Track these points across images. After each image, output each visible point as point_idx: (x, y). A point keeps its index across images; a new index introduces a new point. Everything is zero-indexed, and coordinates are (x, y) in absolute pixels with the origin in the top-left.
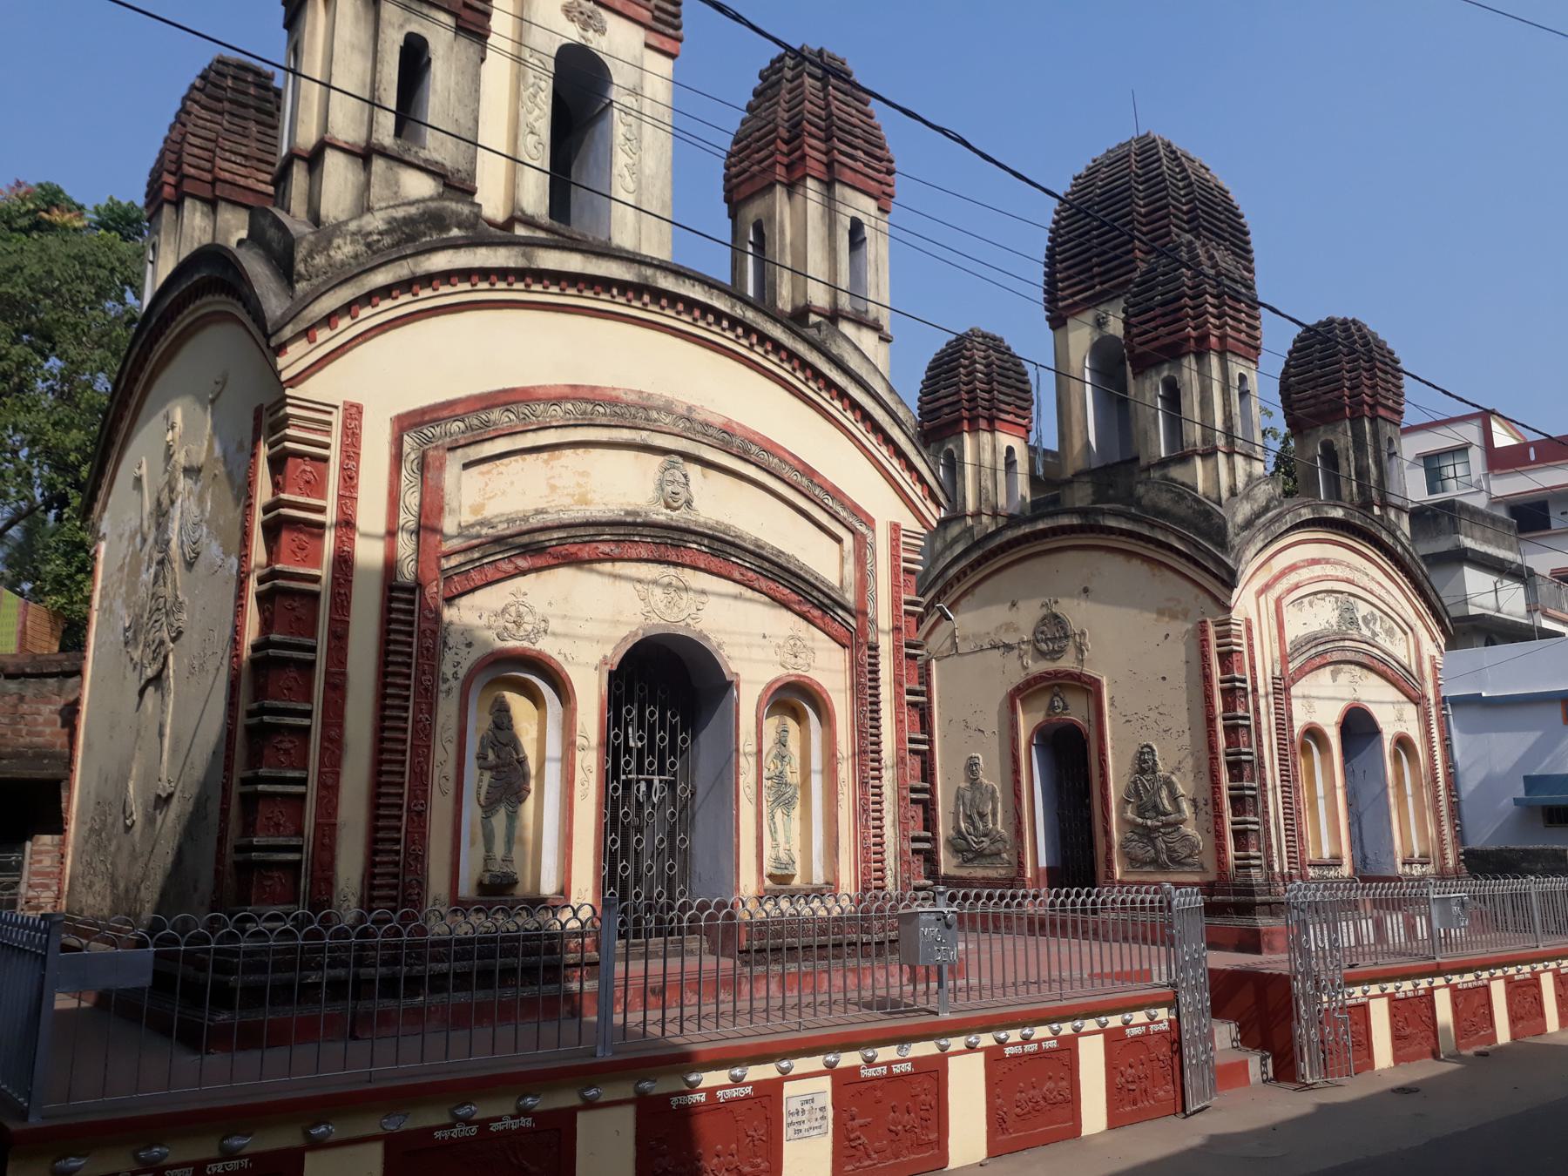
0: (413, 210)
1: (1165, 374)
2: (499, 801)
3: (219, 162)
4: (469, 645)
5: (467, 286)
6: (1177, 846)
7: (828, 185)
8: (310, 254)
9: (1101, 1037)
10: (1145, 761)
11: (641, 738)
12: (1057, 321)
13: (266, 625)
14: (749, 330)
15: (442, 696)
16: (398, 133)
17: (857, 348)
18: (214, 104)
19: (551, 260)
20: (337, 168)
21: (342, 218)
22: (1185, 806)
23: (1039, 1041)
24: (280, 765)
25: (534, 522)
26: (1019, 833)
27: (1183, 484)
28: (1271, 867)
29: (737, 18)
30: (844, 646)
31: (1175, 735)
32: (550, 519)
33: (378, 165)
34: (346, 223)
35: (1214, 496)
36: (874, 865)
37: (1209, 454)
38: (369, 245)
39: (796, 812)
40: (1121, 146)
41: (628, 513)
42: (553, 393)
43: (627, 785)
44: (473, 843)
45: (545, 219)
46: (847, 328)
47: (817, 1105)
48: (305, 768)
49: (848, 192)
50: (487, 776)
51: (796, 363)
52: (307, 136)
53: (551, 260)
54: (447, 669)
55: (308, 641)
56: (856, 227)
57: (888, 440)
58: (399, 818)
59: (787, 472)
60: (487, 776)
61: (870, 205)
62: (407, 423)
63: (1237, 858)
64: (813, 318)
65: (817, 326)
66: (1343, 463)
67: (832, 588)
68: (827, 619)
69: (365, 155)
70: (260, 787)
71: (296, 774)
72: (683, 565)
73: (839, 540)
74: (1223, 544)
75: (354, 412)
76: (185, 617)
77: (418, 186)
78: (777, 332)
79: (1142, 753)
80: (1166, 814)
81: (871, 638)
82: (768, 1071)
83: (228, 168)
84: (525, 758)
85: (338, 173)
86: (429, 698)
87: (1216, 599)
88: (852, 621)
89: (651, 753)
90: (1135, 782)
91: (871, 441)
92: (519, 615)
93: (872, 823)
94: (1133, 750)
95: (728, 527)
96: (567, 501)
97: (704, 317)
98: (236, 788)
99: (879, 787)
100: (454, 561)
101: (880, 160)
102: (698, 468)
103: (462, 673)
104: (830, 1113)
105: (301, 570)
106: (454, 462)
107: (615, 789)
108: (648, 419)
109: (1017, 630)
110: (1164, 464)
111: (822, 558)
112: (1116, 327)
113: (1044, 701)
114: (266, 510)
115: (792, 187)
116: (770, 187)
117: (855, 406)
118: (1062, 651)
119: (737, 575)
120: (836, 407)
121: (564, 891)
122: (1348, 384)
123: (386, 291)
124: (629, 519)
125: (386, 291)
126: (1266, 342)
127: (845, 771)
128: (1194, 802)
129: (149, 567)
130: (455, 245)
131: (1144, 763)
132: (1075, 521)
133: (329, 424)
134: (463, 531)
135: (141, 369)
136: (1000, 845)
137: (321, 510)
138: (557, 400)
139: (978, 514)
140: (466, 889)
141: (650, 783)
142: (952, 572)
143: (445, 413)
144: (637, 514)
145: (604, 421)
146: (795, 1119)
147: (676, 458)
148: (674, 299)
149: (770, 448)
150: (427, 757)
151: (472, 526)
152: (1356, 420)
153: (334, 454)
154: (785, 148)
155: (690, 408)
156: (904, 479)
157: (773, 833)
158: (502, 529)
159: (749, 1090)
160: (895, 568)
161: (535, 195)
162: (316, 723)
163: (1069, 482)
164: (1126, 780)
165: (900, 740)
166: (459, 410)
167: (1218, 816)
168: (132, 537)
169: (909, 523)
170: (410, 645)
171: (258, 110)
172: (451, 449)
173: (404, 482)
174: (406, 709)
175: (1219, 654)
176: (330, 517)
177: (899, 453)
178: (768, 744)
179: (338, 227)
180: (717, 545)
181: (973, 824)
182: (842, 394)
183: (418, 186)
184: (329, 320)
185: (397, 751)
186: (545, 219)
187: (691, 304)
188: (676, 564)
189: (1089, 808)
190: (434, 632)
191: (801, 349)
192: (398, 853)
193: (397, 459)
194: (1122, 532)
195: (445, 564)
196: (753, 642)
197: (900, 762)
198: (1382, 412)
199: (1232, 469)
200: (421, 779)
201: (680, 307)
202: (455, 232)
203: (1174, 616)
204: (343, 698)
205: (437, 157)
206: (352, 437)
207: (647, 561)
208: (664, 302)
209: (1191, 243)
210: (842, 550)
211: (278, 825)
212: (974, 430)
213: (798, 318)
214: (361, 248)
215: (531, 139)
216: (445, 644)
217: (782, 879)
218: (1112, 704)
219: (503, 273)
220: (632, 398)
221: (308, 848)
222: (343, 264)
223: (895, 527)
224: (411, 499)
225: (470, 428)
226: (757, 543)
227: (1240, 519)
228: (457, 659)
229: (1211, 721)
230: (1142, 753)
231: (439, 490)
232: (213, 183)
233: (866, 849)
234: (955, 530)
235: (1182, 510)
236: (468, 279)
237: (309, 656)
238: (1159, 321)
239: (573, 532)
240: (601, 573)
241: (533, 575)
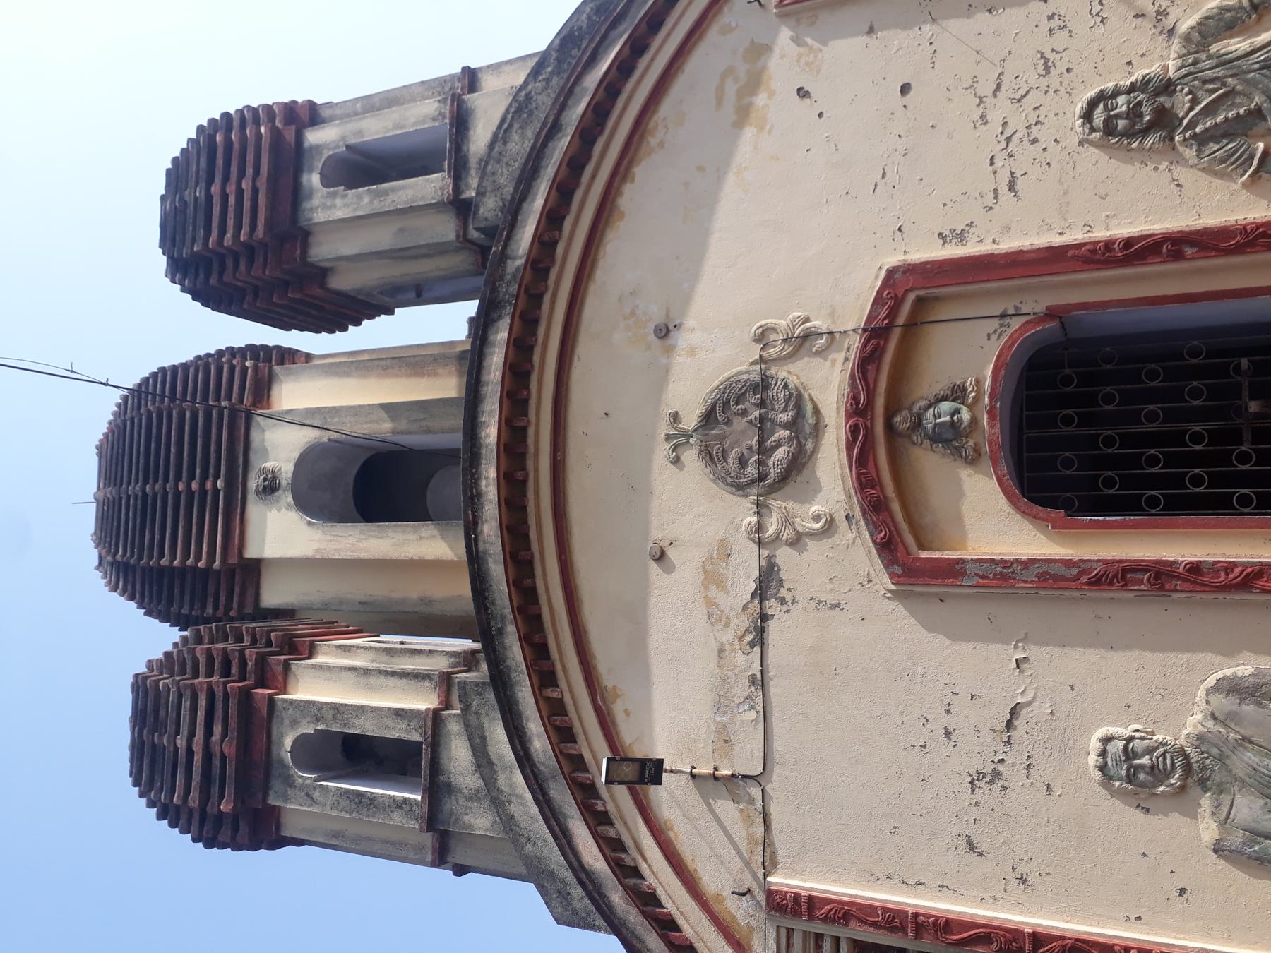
1: (315, 179)
10: (1134, 113)
31: (1061, 39)
90: (1201, 140)
94: (1098, 164)
113: (930, 464)
118: (797, 400)
142: (540, 744)
164: (1191, 178)
203: (754, 83)
218: (961, 237)
230: (1109, 129)
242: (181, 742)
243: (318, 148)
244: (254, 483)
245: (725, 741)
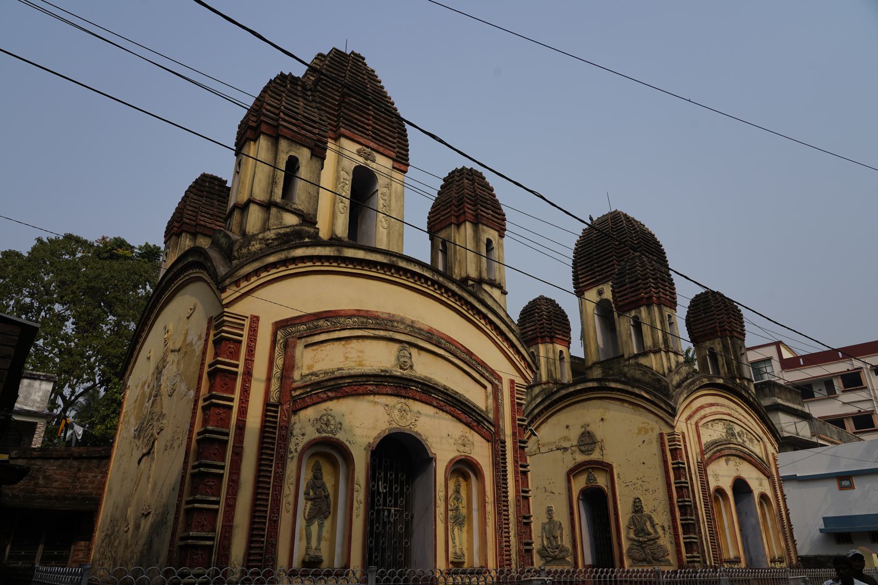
0: (288, 230)
2: (314, 517)
3: (199, 217)
4: (303, 435)
5: (311, 264)
6: (656, 551)
7: (475, 224)
8: (240, 248)
11: (385, 488)
12: (580, 292)
13: (205, 422)
14: (441, 286)
15: (289, 460)
16: (283, 197)
17: (491, 296)
18: (199, 193)
19: (350, 253)
20: (255, 212)
21: (256, 232)
22: (659, 530)
24: (207, 494)
25: (337, 374)
26: (574, 546)
27: (646, 366)
28: (705, 562)
29: (441, 141)
30: (488, 441)
32: (345, 372)
33: (274, 211)
34: (257, 235)
35: (661, 372)
36: (505, 557)
37: (657, 351)
38: (267, 245)
39: (465, 529)
40: (604, 216)
41: (382, 371)
42: (349, 313)
44: (300, 540)
45: (346, 239)
46: (487, 288)
48: (219, 496)
49: (485, 228)
50: (309, 503)
52: (245, 197)
53: (350, 253)
54: (292, 447)
55: (225, 430)
56: (489, 242)
57: (507, 339)
58: (265, 523)
59: (459, 353)
60: (309, 503)
61: (496, 234)
62: (280, 325)
63: (687, 557)
64: (470, 282)
65: (472, 286)
66: (720, 358)
67: (482, 411)
68: (480, 427)
69: (267, 206)
70: (196, 505)
71: (215, 499)
72: (409, 398)
73: (485, 387)
74: (668, 395)
75: (255, 320)
76: (165, 421)
77: (291, 220)
78: (454, 288)
79: (635, 502)
80: (650, 534)
81: (502, 437)
83: (203, 220)
84: (329, 495)
85: (255, 215)
86: (282, 462)
87: (667, 422)
88: (492, 428)
89: (391, 495)
91: (499, 340)
92: (328, 420)
93: (504, 535)
95: (431, 379)
96: (353, 364)
97: (420, 280)
98: (184, 506)
99: (508, 515)
100: (298, 393)
101: (499, 214)
103: (299, 449)
105: (225, 395)
107: (372, 514)
108: (392, 326)
109: (569, 440)
110: (636, 356)
111: (476, 395)
112: (608, 294)
114: (210, 366)
115: (458, 226)
116: (450, 225)
117: (491, 322)
119: (435, 403)
120: (482, 323)
121: (347, 566)
123: (274, 265)
124: (383, 374)
125: (274, 265)
126: (679, 300)
127: (490, 508)
128: (663, 528)
129: (149, 399)
130: (307, 245)
131: (637, 507)
132: (595, 384)
133: (243, 325)
134: (303, 376)
135: (155, 307)
136: (564, 553)
137: (237, 366)
138: (350, 316)
139: (547, 383)
140: (296, 564)
141: (389, 511)
142: (536, 411)
143: (298, 321)
144: (386, 371)
145: (372, 326)
147: (406, 345)
148: (406, 271)
149: (451, 341)
150: (280, 492)
151: (308, 375)
153: (245, 340)
154: (456, 209)
155: (412, 321)
156: (516, 358)
157: (453, 539)
158: (322, 377)
160: (512, 402)
161: (342, 229)
162: (226, 472)
163: (591, 368)
165: (517, 491)
166: (304, 320)
167: (676, 536)
168: (143, 386)
169: (519, 380)
170: (275, 433)
171: (219, 196)
172: (300, 338)
173: (276, 354)
174: (271, 466)
175: (670, 450)
176: (240, 370)
177: (512, 345)
178: (450, 492)
179: (254, 235)
180: (425, 388)
181: (550, 542)
182: (485, 317)
183: (291, 220)
184: (247, 277)
185: (264, 494)
186: (346, 239)
187: (414, 274)
188: (405, 397)
189: (610, 532)
190: (286, 427)
191: (465, 295)
192: (263, 542)
193: (274, 342)
194: (618, 390)
195: (294, 394)
196: (443, 437)
198: (735, 334)
199: (669, 359)
200: (277, 502)
201: (409, 275)
202: (307, 240)
204: (241, 460)
205: (300, 208)
206: (253, 331)
207: (391, 395)
208: (401, 273)
209: (640, 256)
210: (486, 392)
211: (203, 525)
212: (544, 342)
213: (463, 282)
214: (263, 246)
215: (341, 205)
216: (292, 434)
217: (458, 564)
220: (385, 316)
221: (218, 538)
222: (255, 252)
224: (279, 362)
225: (309, 328)
226: (445, 387)
227: (674, 383)
228: (297, 441)
229: (669, 485)
231: (293, 357)
232: (196, 226)
233: (501, 548)
234: (537, 390)
235: (646, 379)
236: (312, 261)
237: (225, 438)
238: (629, 290)
239: (355, 380)
240: (369, 401)
241: (335, 401)
242: (527, 325)
243: (640, 312)
244: (600, 287)
245: (543, 445)
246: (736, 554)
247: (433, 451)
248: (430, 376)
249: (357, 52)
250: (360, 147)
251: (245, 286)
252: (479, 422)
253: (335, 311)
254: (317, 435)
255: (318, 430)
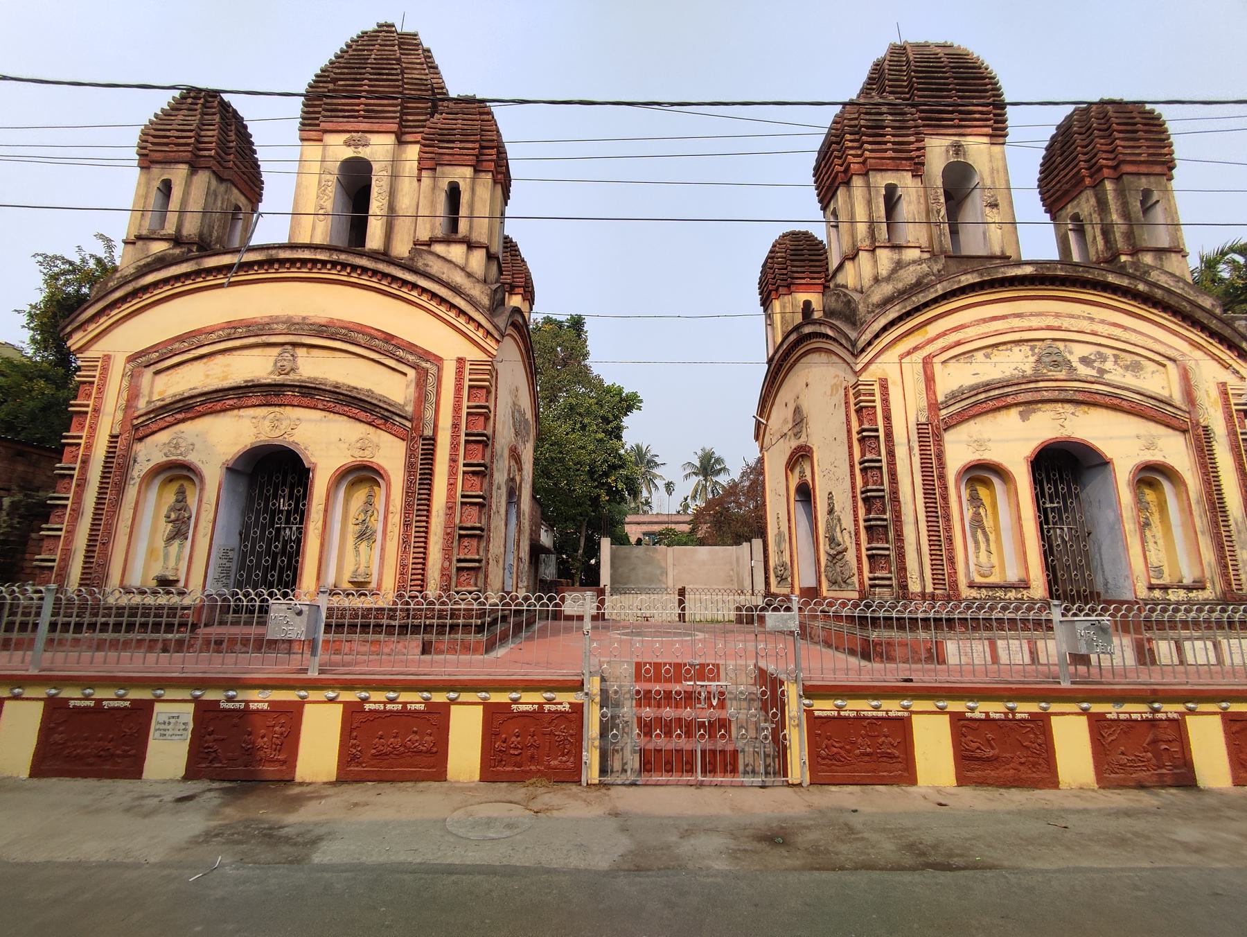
9: (481, 707)
14: (344, 266)
23: (404, 704)
28: (904, 586)
43: (278, 530)
47: (182, 720)
51: (379, 276)
62: (132, 358)
63: (871, 579)
66: (1088, 228)
75: (107, 358)
82: (146, 695)
91: (441, 310)
95: (316, 379)
100: (140, 420)
102: (305, 350)
104: (191, 726)
106: (148, 373)
111: (394, 387)
120: (413, 295)
122: (1081, 157)
146: (162, 727)
148: (293, 262)
152: (1097, 186)
155: (304, 318)
156: (470, 329)
159: (127, 704)
169: (474, 354)
182: (414, 286)
187: (304, 262)
188: (280, 405)
196: (326, 442)
197: (450, 508)
219: (187, 275)
220: (267, 320)
223: (461, 361)
246: (1023, 575)
247: (313, 460)
248: (321, 376)
249: (383, 22)
250: (347, 136)
251: (94, 330)
252: (386, 419)
253: (198, 330)
254: (165, 459)
255: (166, 455)
